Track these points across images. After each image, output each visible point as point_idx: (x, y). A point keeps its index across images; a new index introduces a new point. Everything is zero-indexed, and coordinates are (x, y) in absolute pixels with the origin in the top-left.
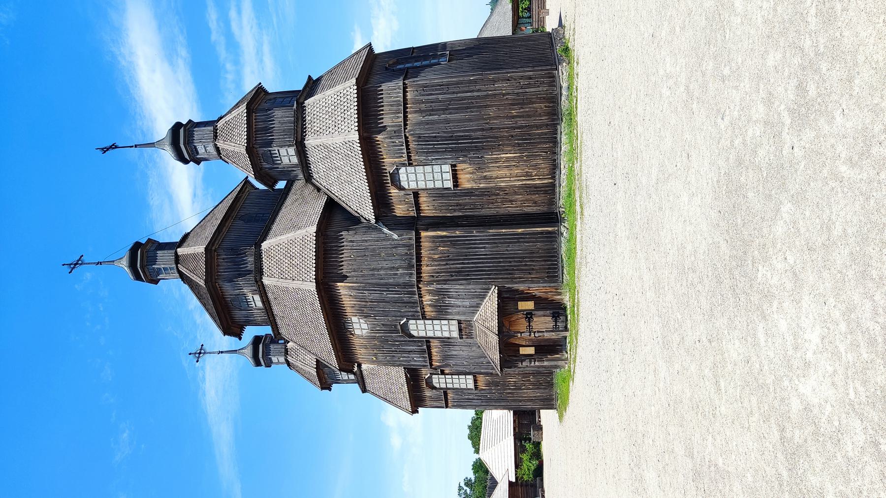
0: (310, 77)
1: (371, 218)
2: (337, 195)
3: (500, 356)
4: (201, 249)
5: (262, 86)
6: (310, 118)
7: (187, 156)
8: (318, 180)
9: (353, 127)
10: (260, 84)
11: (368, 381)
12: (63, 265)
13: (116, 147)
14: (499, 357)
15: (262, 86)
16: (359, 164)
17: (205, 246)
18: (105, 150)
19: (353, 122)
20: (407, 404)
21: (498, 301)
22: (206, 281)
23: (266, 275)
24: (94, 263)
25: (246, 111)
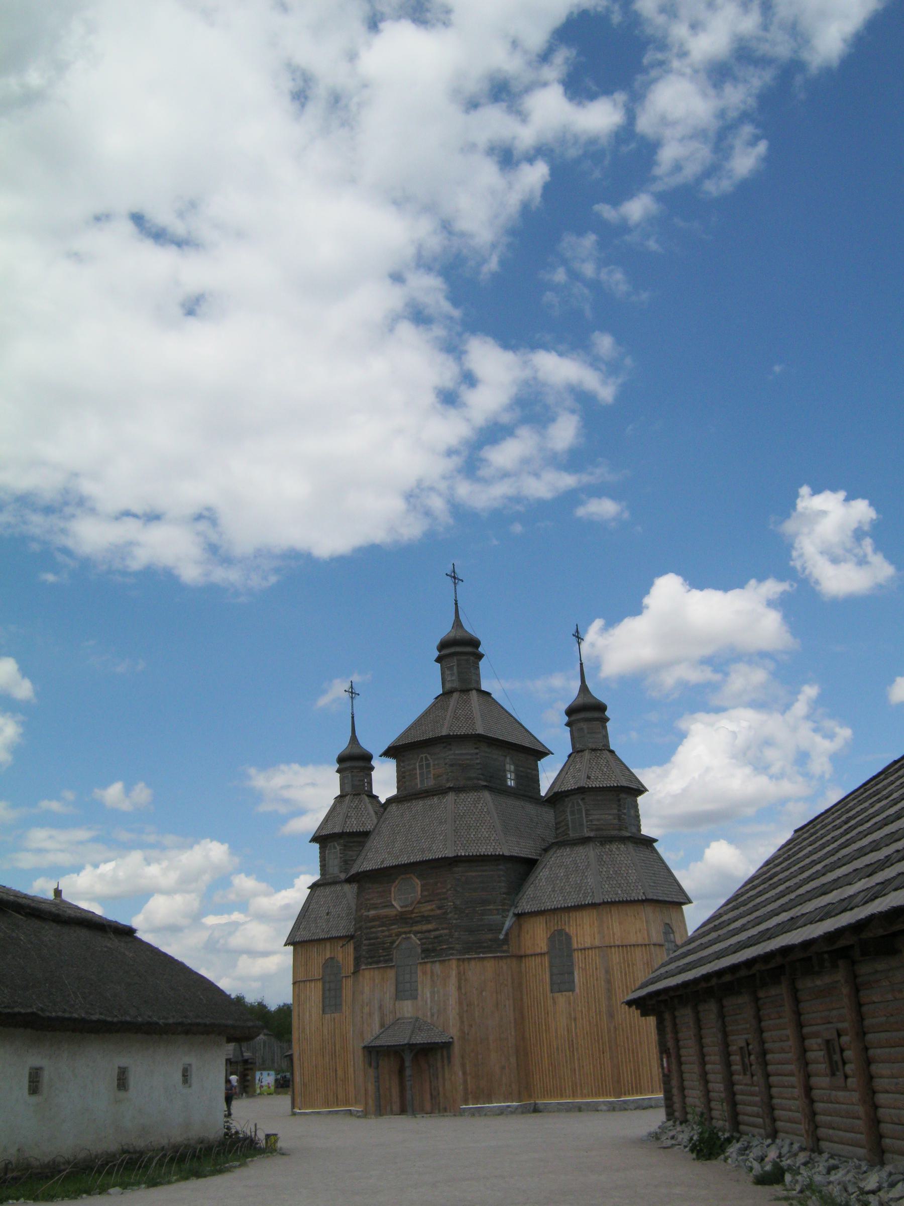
0: (655, 840)
1: (519, 908)
2: (541, 874)
4: (480, 731)
6: (614, 849)
8: (555, 855)
9: (607, 897)
11: (328, 890)
12: (453, 564)
14: (384, 1044)
16: (572, 900)
19: (611, 896)
20: (304, 935)
21: (442, 1042)
23: (456, 798)
24: (456, 597)
25: (619, 785)
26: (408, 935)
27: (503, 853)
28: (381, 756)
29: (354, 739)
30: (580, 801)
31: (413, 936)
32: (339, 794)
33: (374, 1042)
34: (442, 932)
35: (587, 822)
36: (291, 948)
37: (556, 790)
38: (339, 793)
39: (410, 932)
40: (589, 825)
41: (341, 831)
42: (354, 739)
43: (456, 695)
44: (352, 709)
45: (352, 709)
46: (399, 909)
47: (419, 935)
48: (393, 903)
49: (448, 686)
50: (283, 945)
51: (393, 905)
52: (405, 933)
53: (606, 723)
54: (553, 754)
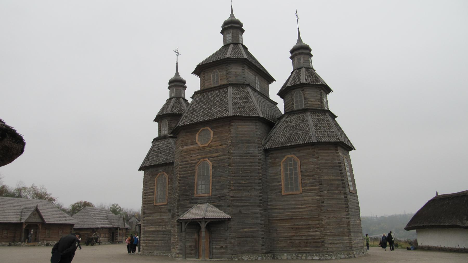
0: (337, 117)
3: (190, 219)
5: (331, 92)
7: (294, 53)
10: (333, 91)
13: (298, 19)
15: (331, 92)
17: (247, 58)
18: (296, 14)
21: (223, 218)
22: (228, 58)
24: (232, 4)
26: (205, 159)
27: (259, 116)
28: (192, 73)
29: (177, 73)
30: (301, 91)
31: (207, 159)
32: (169, 98)
33: (183, 217)
34: (224, 157)
35: (305, 102)
36: (142, 173)
37: (288, 85)
38: (169, 98)
39: (206, 158)
40: (306, 104)
41: (169, 113)
42: (177, 73)
43: (231, 46)
44: (177, 60)
45: (177, 60)
46: (201, 146)
47: (211, 159)
48: (197, 142)
49: (228, 42)
50: (138, 169)
51: (197, 144)
52: (204, 158)
53: (311, 57)
54: (275, 81)
